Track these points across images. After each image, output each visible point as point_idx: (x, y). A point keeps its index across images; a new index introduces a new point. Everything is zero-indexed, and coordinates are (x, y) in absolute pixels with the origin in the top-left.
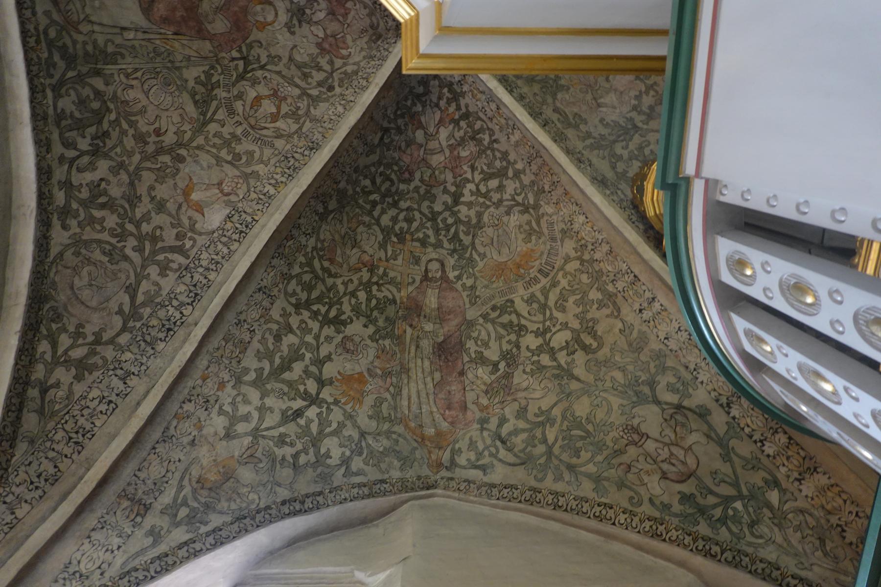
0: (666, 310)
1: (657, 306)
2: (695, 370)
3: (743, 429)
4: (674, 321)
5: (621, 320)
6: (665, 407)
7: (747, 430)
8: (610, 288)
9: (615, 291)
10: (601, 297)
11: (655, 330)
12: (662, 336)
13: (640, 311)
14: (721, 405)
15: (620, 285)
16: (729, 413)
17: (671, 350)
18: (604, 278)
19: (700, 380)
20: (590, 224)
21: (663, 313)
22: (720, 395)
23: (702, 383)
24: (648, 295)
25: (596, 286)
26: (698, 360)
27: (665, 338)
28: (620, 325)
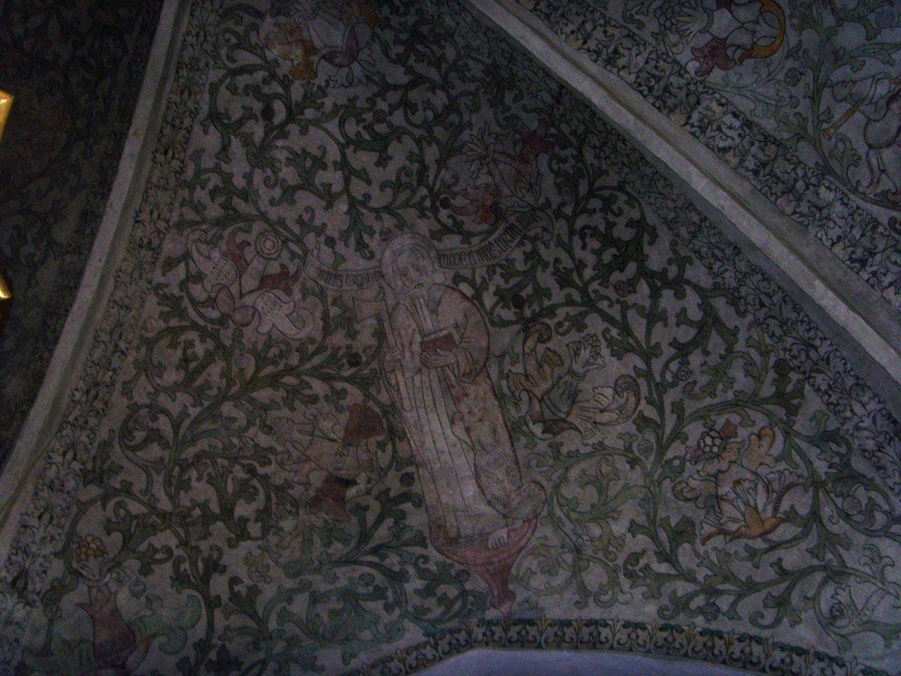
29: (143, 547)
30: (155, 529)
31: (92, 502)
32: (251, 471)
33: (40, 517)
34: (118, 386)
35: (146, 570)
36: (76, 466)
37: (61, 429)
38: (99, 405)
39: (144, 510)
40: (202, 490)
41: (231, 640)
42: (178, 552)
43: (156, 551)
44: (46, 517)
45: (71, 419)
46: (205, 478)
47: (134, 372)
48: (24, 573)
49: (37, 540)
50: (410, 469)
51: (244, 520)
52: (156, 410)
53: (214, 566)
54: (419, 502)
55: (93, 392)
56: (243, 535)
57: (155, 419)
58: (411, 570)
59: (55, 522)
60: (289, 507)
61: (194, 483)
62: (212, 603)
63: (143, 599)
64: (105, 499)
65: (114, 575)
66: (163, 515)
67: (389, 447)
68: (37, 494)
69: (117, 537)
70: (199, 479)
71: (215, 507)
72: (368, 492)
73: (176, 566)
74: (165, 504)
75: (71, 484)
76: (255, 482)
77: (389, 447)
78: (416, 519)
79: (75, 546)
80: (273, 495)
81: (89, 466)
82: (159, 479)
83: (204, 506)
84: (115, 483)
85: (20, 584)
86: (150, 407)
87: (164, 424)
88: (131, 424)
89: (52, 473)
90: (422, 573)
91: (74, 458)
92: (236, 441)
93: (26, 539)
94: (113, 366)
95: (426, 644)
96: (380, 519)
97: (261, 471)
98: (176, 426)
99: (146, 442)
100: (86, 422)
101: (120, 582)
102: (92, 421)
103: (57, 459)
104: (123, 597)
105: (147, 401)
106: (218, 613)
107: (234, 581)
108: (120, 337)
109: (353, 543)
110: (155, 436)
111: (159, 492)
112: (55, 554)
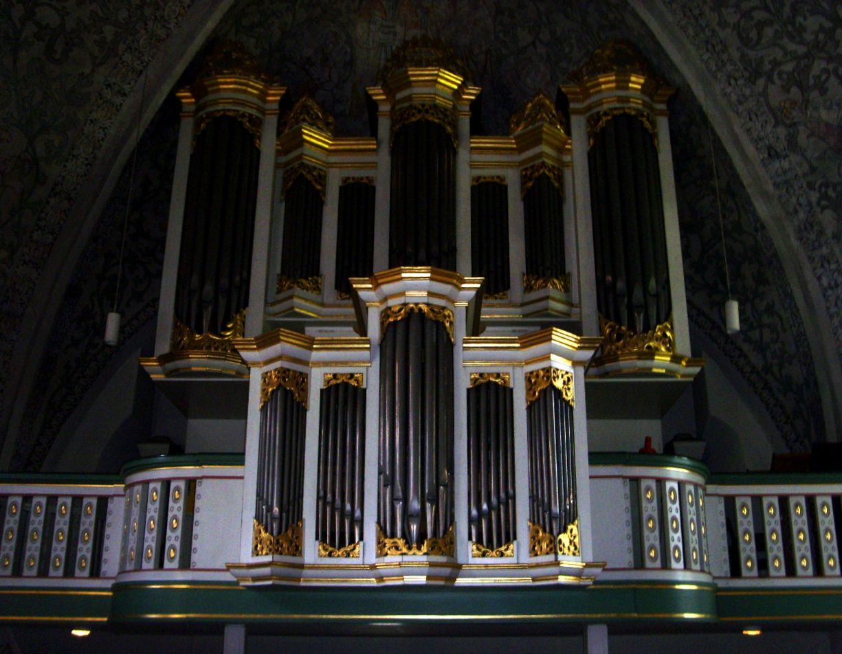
0: (118, 110)
1: (118, 100)
2: (74, 156)
3: (42, 212)
4: (110, 121)
5: (93, 71)
6: (30, 150)
7: (43, 215)
8: (122, 47)
9: (120, 53)
10: (108, 40)
11: (95, 108)
12: (94, 116)
13: (109, 86)
14: (53, 189)
15: (128, 57)
16: (50, 196)
17: (83, 130)
18: (130, 38)
19: (67, 164)
20: (183, 11)
21: (114, 108)
22: (62, 184)
23: (65, 166)
24: (127, 88)
25: (119, 30)
26: (83, 155)
27: (91, 121)
28: (87, 71)
29: (812, 82)
30: (808, 68)
31: (766, 87)
33: (750, 119)
34: (717, 28)
35: (823, 91)
36: (741, 82)
37: (716, 78)
38: (719, 47)
39: (795, 63)
42: (831, 67)
43: (819, 77)
44: (754, 117)
45: (714, 68)
46: (808, 15)
47: (716, 14)
48: (770, 148)
49: (760, 129)
52: (747, 15)
55: (710, 47)
57: (752, 18)
59: (759, 114)
61: (804, 24)
64: (770, 79)
66: (807, 55)
68: (737, 113)
69: (794, 90)
70: (805, 19)
74: (801, 50)
75: (747, 92)
79: (779, 114)
81: (747, 74)
82: (785, 41)
83: (822, 29)
84: (767, 67)
85: (773, 153)
86: (742, 16)
87: (759, 15)
88: (744, 35)
89: (734, 98)
91: (736, 80)
93: (755, 135)
94: (704, 25)
98: (767, 9)
99: (760, 35)
100: (722, 61)
102: (725, 57)
103: (729, 90)
104: (824, 114)
105: (739, 16)
108: (691, 11)
110: (760, 26)
111: (791, 47)
112: (775, 127)
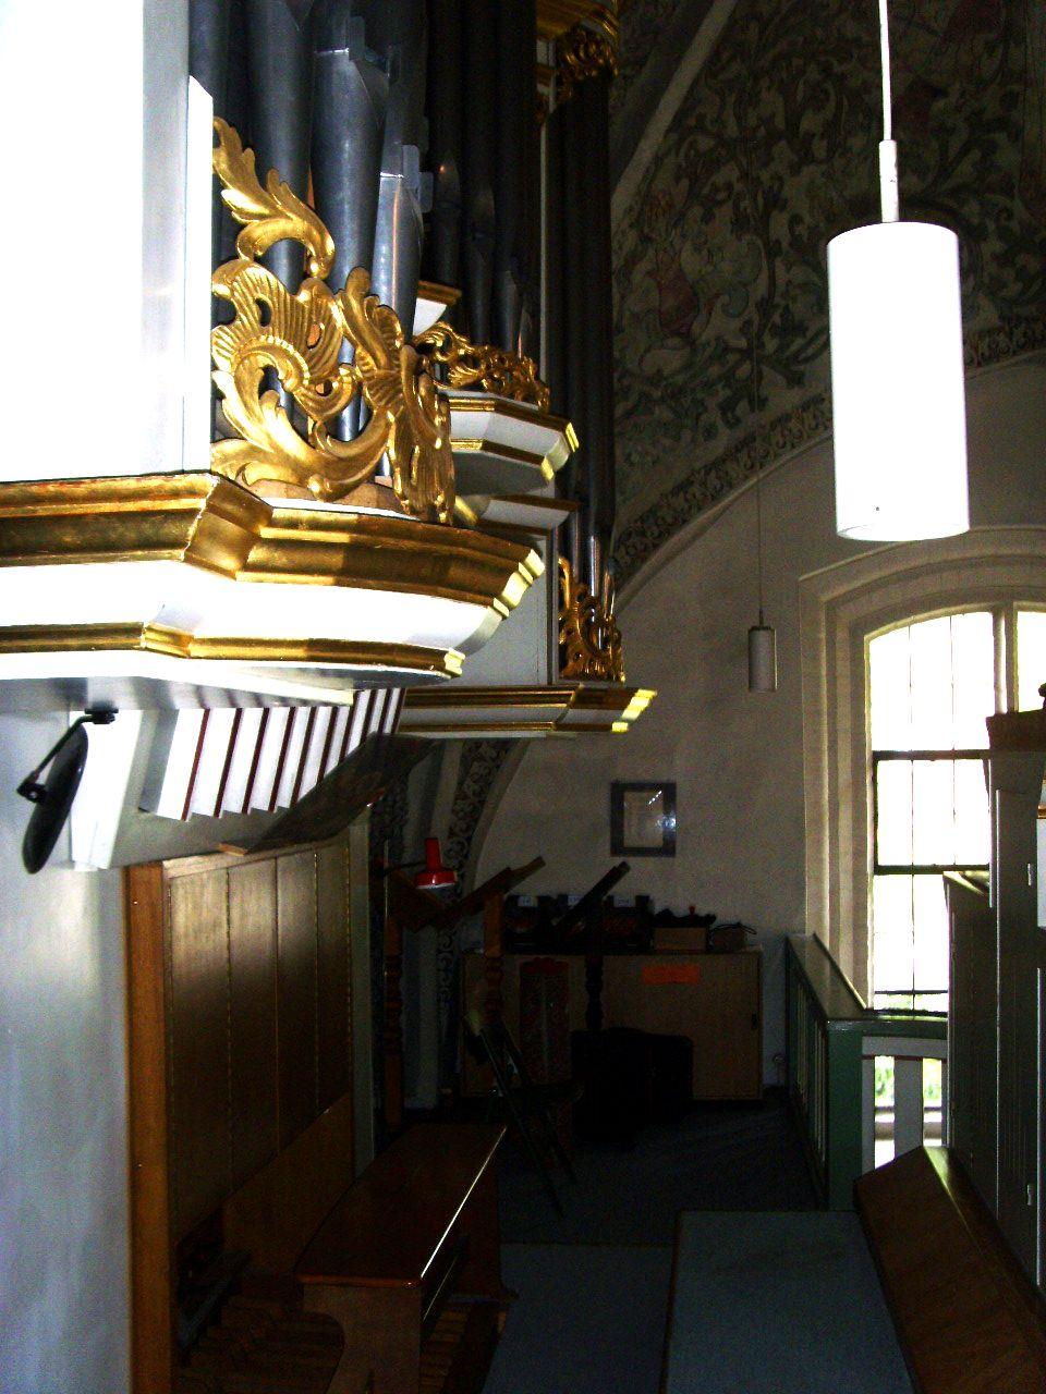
29: (706, 191)
32: (827, 70)
40: (772, 103)
41: (794, 299)
43: (717, 190)
50: (1015, 87)
51: (810, 136)
53: (775, 202)
54: (1016, 135)
56: (806, 157)
58: (991, 226)
60: (860, 118)
62: (773, 250)
63: (705, 252)
65: (679, 230)
67: (999, 53)
71: (780, 123)
72: (958, 109)
73: (736, 207)
76: (828, 86)
77: (999, 53)
78: (1008, 157)
80: (845, 102)
90: (1003, 233)
92: (819, 33)
95: (1000, 330)
96: (965, 151)
97: (838, 68)
101: (684, 236)
106: (778, 262)
107: (796, 220)
109: (930, 179)
